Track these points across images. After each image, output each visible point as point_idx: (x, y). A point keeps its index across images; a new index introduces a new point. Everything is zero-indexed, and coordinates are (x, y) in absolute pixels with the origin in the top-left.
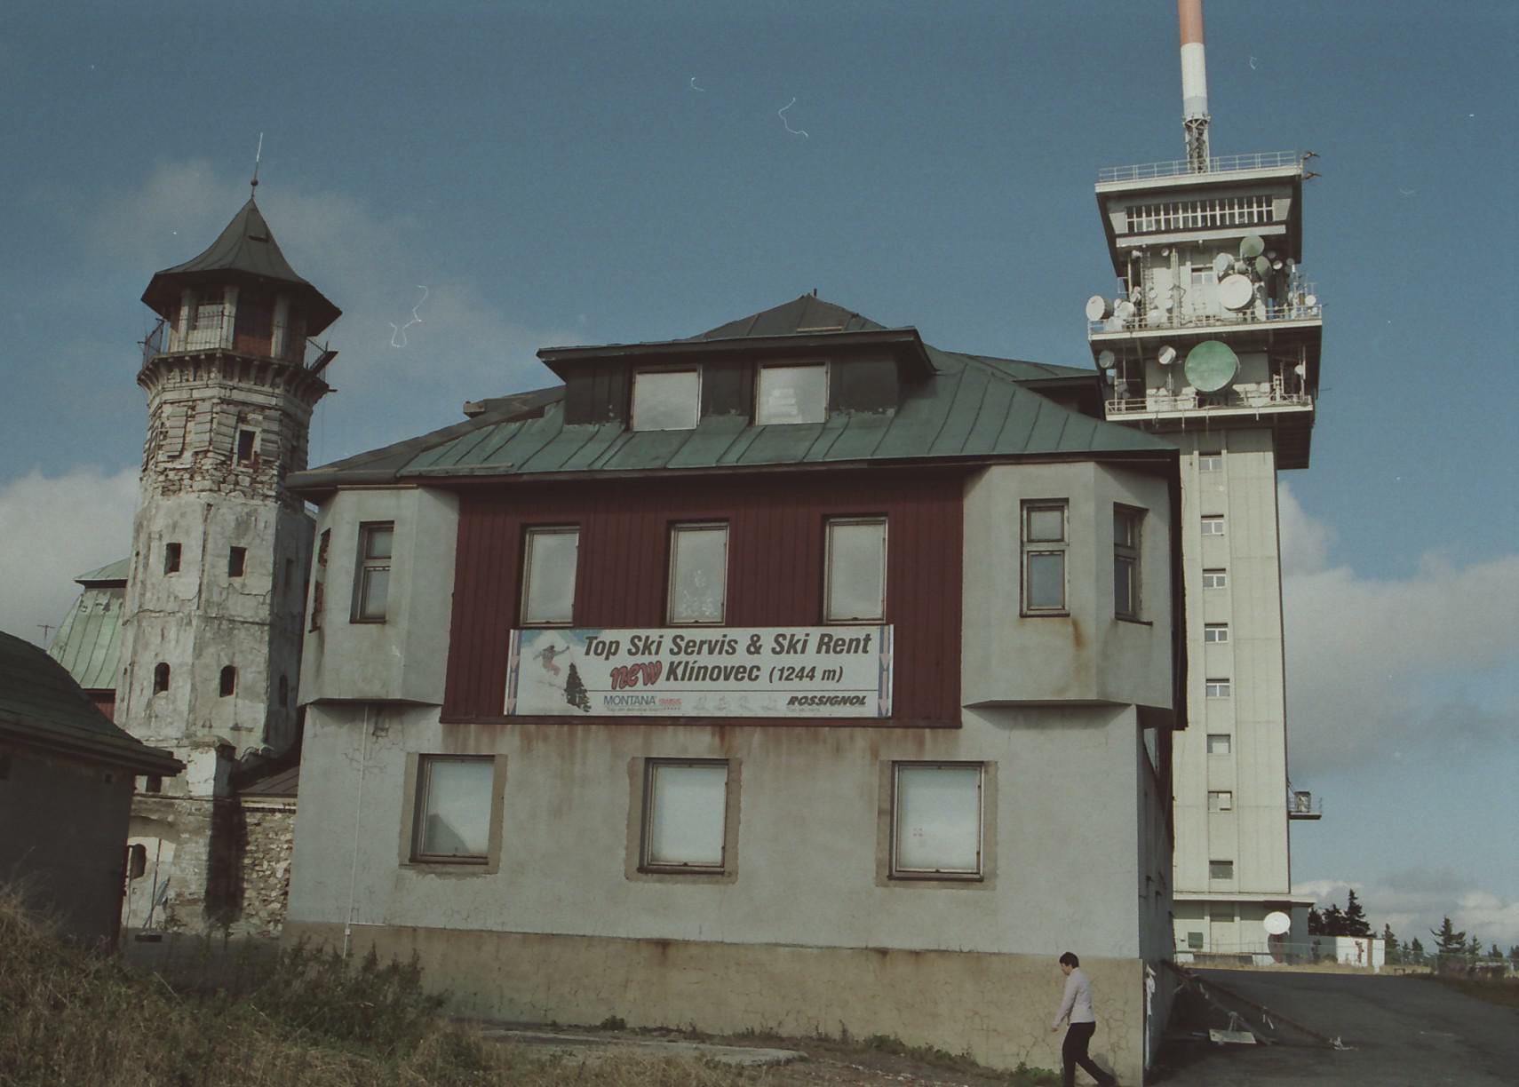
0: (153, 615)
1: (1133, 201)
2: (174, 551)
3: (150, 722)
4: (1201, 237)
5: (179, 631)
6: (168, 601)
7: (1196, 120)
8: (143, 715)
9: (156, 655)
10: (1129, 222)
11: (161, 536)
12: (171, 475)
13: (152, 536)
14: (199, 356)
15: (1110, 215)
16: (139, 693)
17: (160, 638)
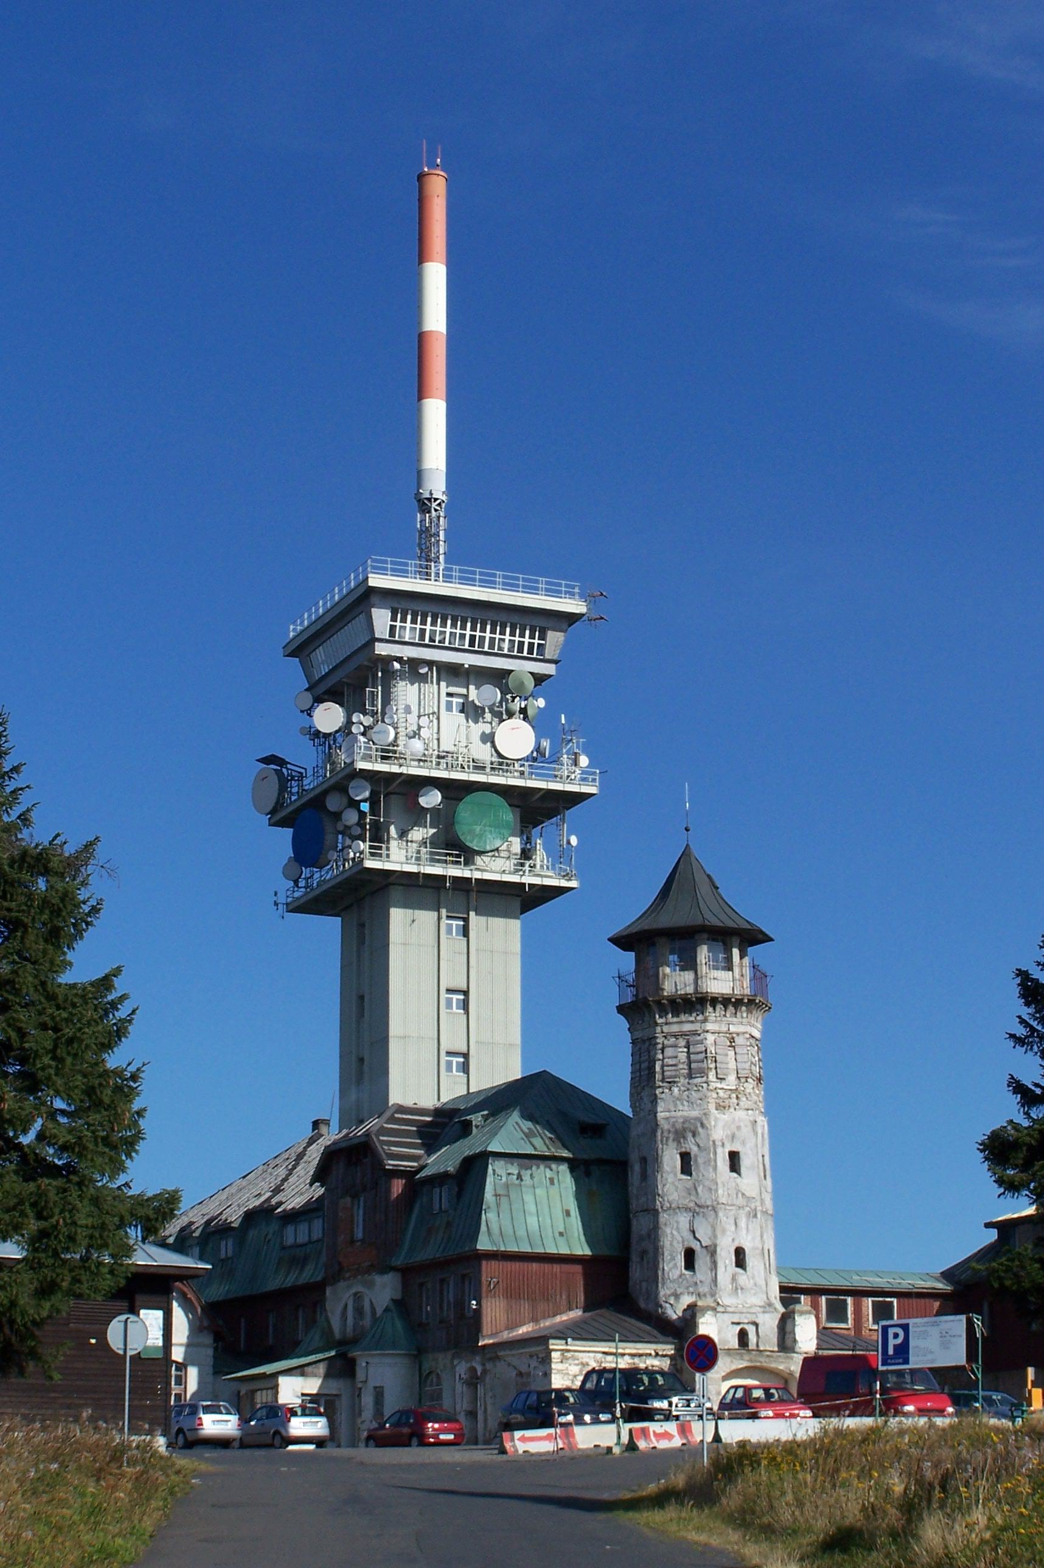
0: (728, 1208)
1: (399, 601)
2: (734, 1157)
3: (737, 1293)
4: (468, 660)
6: (737, 1197)
7: (436, 500)
8: (730, 1286)
9: (733, 1240)
10: (391, 625)
11: (723, 1145)
12: (721, 1093)
13: (717, 1143)
14: (743, 999)
15: (373, 609)
16: (723, 1270)
17: (733, 1228)
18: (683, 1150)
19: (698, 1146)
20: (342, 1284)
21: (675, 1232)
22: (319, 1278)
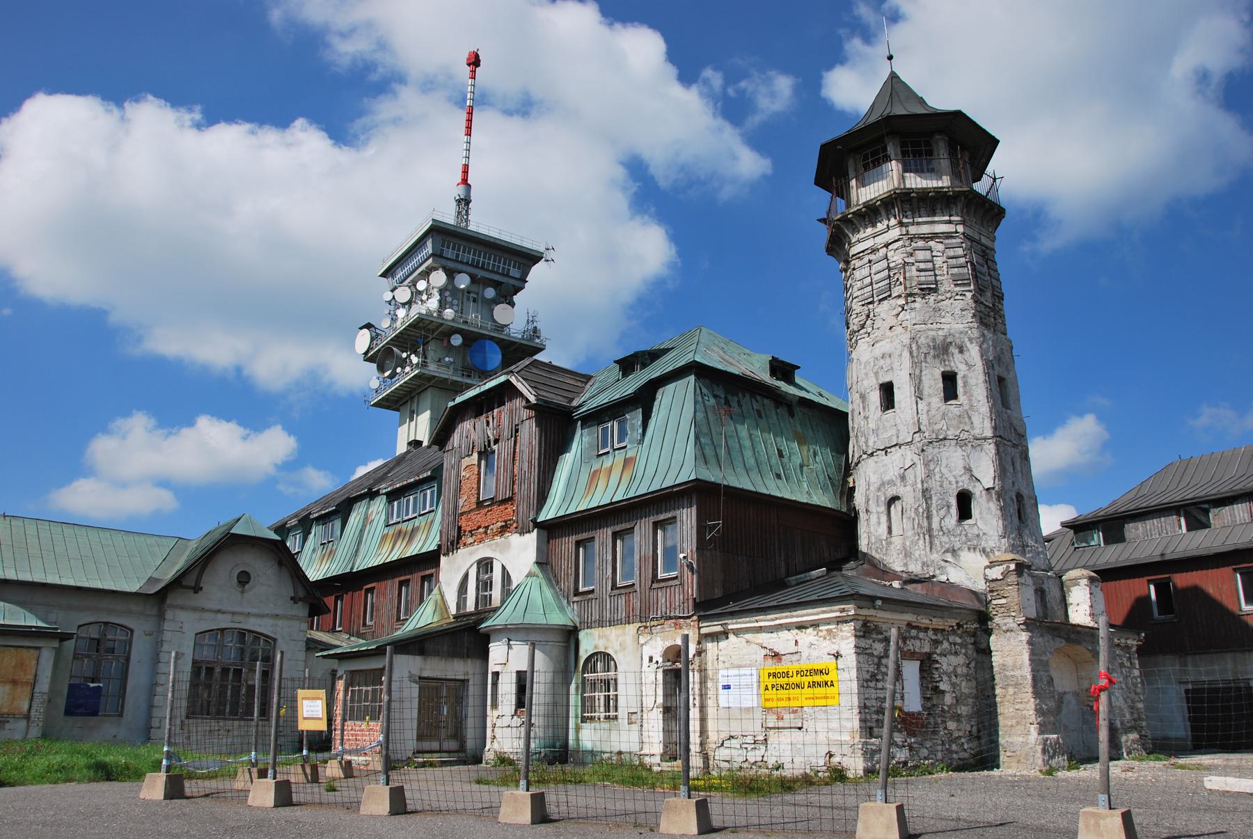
5: (1021, 463)
9: (1013, 483)
18: (948, 369)
19: (967, 364)
20: (462, 551)
21: (945, 471)
22: (433, 547)
